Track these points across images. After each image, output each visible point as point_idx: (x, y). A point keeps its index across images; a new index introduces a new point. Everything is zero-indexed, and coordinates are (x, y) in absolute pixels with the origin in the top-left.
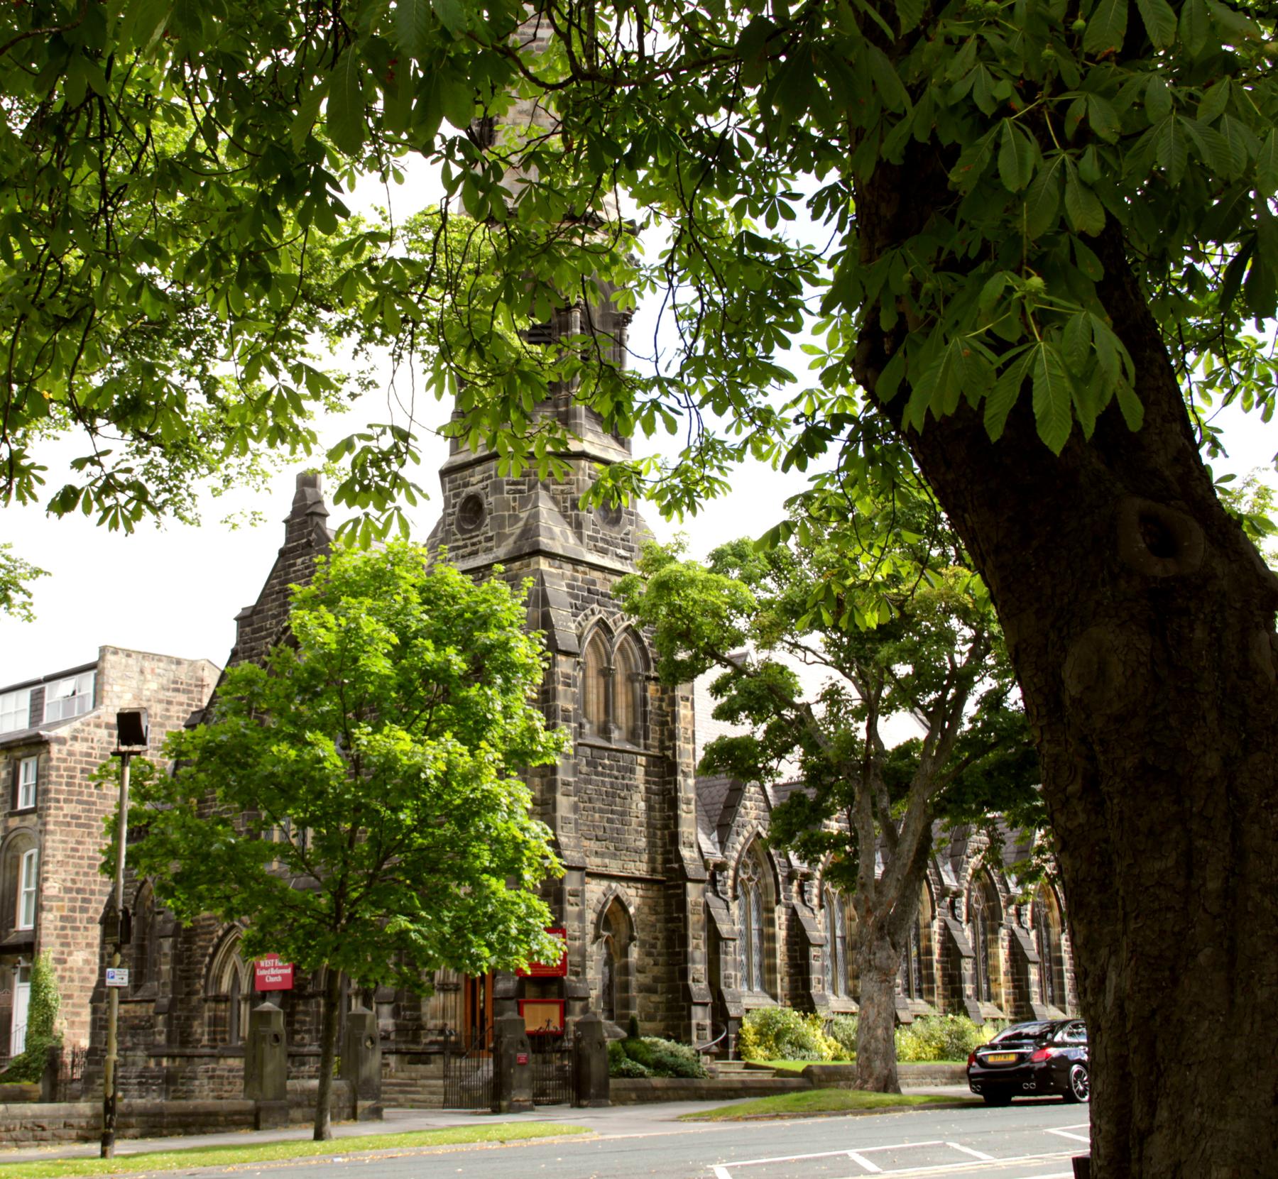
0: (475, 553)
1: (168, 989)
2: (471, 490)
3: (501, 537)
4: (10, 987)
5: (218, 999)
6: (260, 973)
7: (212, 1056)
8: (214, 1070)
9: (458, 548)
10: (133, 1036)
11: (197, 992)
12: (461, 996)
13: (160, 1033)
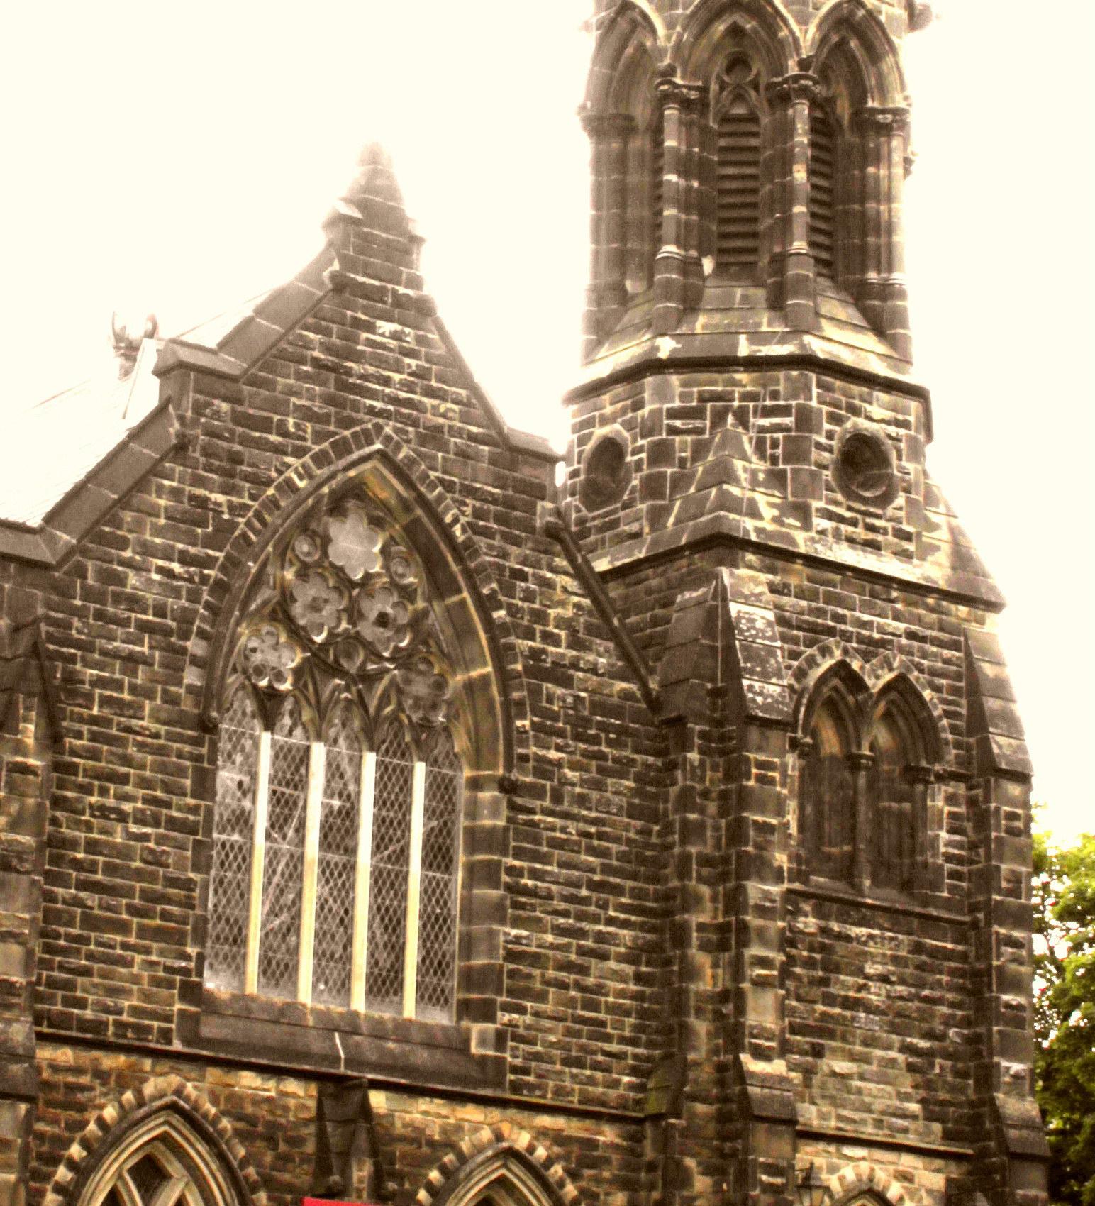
2: (863, 423)
9: (841, 519)
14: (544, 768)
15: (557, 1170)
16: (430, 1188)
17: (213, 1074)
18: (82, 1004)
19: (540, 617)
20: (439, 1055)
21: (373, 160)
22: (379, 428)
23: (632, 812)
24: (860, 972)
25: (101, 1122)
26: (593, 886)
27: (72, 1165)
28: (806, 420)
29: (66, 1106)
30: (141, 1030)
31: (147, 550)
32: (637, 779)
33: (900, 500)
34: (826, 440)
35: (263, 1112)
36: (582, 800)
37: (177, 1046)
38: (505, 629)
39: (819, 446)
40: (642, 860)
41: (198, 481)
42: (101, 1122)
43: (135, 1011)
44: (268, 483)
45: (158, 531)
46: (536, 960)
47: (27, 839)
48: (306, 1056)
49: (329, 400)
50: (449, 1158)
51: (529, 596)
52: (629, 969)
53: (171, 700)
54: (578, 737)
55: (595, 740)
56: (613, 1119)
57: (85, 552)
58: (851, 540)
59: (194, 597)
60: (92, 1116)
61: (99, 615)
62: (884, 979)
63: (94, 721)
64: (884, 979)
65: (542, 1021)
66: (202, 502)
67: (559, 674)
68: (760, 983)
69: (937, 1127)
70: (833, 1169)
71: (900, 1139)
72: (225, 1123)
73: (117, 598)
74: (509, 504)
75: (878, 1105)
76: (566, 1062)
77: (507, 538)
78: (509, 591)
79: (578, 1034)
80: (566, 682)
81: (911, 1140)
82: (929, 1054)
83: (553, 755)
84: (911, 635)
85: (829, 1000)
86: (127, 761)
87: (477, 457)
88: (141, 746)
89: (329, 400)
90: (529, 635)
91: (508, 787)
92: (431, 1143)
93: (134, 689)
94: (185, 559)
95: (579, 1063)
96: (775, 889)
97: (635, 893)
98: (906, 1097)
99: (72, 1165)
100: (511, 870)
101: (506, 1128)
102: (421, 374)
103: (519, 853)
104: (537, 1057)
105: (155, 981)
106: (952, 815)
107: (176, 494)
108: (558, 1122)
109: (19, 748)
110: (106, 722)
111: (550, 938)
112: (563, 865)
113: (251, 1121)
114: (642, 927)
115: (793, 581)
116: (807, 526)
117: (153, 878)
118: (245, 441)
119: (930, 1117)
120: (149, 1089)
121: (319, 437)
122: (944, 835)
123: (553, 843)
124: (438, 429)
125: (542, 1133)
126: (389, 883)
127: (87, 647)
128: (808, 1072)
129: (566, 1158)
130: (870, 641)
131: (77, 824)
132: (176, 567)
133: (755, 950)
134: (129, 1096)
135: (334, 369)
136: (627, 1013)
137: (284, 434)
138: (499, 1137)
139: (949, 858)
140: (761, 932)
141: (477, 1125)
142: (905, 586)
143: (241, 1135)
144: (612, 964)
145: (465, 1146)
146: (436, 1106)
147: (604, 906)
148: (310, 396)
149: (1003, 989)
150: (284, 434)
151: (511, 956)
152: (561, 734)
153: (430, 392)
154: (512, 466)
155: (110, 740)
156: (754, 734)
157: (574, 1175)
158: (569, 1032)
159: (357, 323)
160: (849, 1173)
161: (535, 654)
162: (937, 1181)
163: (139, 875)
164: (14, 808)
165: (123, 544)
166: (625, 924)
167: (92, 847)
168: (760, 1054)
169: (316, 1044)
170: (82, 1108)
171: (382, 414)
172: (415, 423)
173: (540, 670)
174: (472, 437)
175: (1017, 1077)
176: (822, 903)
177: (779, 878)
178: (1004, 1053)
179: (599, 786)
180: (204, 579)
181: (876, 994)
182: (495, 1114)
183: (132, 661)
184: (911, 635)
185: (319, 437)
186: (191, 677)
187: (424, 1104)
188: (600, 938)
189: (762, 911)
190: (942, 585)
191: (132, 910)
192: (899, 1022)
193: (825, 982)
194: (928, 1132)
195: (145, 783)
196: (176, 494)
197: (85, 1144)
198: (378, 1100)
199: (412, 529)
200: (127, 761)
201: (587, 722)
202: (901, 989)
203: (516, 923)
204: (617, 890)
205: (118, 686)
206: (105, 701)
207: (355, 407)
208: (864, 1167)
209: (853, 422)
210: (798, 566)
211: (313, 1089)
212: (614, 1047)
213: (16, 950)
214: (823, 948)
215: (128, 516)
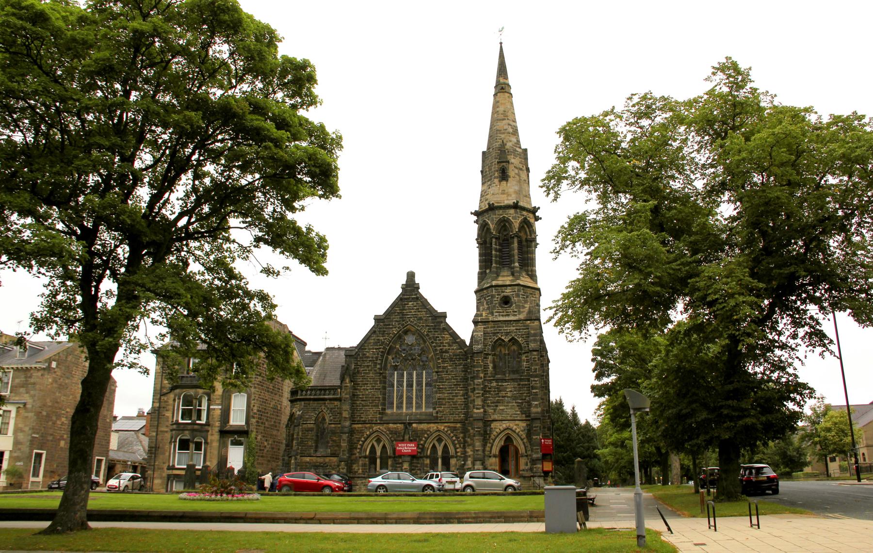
1: (346, 453)
2: (505, 294)
3: (520, 312)
4: (227, 447)
5: (365, 457)
14: (444, 368)
21: (411, 276)
28: (493, 296)
34: (497, 300)
67: (446, 352)
91: (437, 372)
126: (420, 391)
128: (495, 410)
141: (433, 427)
148: (397, 318)
160: (504, 426)
162: (525, 425)
168: (477, 409)
169: (403, 418)
173: (442, 352)
176: (497, 381)
181: (509, 394)
183: (368, 366)
186: (378, 366)
192: (514, 398)
198: (414, 425)
209: (502, 294)
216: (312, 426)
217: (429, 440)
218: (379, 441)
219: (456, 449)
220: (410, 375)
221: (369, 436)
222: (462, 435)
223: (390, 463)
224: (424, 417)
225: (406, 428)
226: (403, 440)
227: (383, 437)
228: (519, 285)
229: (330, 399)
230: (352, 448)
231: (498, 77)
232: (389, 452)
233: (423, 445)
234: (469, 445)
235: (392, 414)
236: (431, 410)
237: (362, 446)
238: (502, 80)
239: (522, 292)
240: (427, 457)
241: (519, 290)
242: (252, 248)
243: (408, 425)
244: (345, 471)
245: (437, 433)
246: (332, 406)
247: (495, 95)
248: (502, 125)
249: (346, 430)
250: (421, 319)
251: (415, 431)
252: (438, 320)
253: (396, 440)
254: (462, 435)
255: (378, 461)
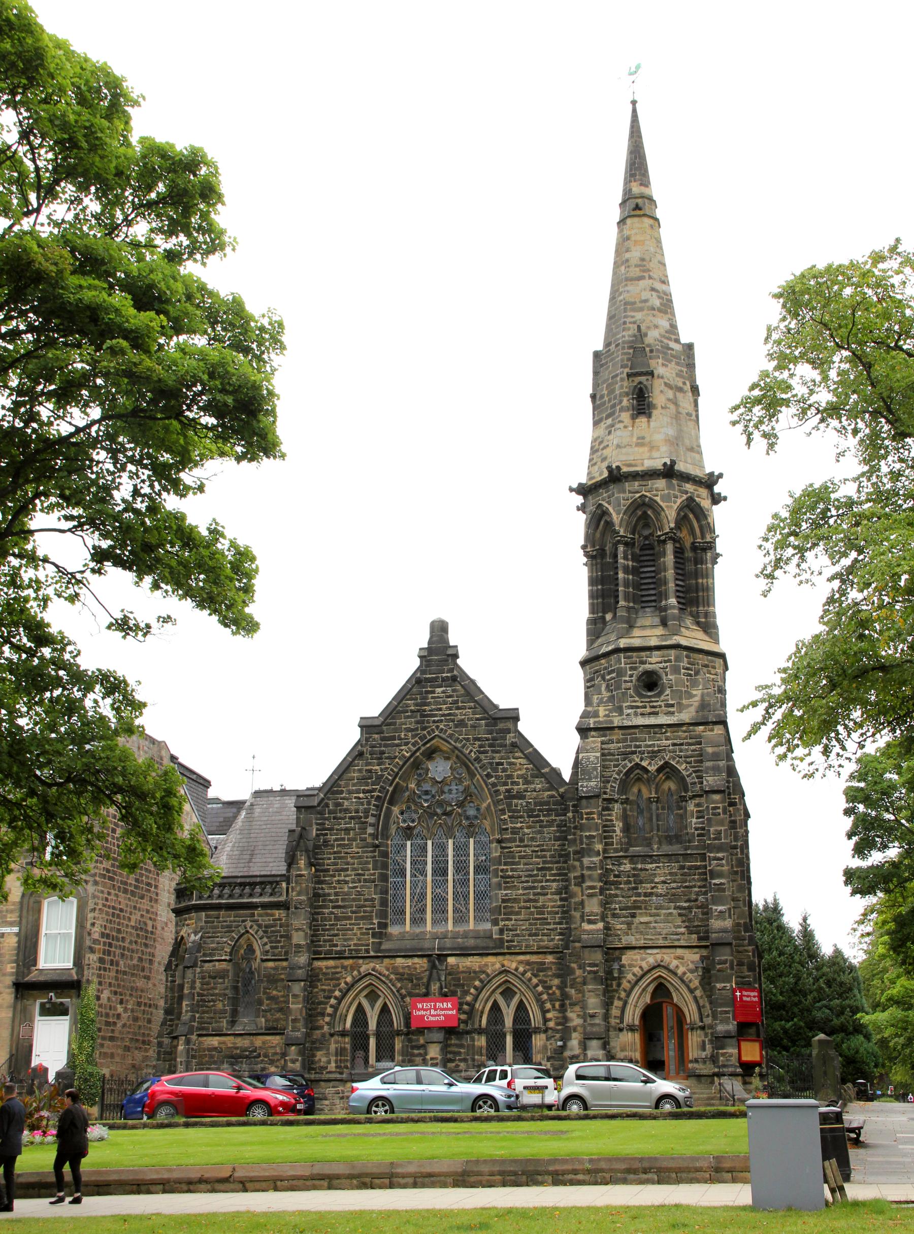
0: (656, 713)
1: (300, 1025)
3: (681, 707)
4: (32, 1020)
5: (343, 1034)
6: (416, 1013)
7: (341, 1080)
8: (343, 1092)
9: (638, 707)
10: (232, 1064)
11: (322, 1027)
12: (637, 1036)
13: (293, 1061)
14: (515, 831)
15: (529, 974)
16: (476, 988)
17: (386, 961)
18: (336, 945)
19: (510, 777)
20: (478, 941)
21: (439, 630)
22: (437, 727)
23: (557, 839)
24: (652, 882)
25: (346, 983)
26: (539, 869)
27: (336, 998)
28: (620, 673)
29: (331, 979)
30: (356, 950)
31: (350, 792)
32: (558, 826)
33: (668, 692)
34: (630, 679)
35: (407, 971)
36: (532, 839)
37: (372, 954)
38: (494, 785)
39: (626, 681)
40: (560, 856)
41: (368, 764)
42: (346, 983)
43: (355, 945)
44: (395, 757)
45: (354, 785)
46: (515, 900)
47: (303, 898)
48: (421, 950)
49: (417, 722)
50: (483, 976)
51: (504, 770)
52: (557, 897)
53: (363, 840)
54: (529, 817)
55: (538, 816)
56: (551, 953)
57: (329, 799)
58: (642, 714)
59: (369, 803)
60: (342, 981)
61: (334, 818)
62: (664, 882)
63: (335, 853)
64: (664, 882)
65: (520, 923)
66: (370, 771)
67: (520, 796)
68: (591, 896)
69: (694, 936)
70: (643, 959)
71: (677, 944)
72: (392, 976)
73: (341, 811)
74: (494, 739)
75: (664, 932)
76: (530, 935)
77: (493, 752)
78: (496, 770)
79: (536, 924)
80: (522, 797)
81: (683, 943)
82: (689, 908)
83: (519, 825)
84: (674, 745)
85: (639, 895)
86: (348, 864)
87: (480, 726)
88: (352, 858)
89: (417, 722)
90: (505, 784)
91: (499, 841)
92: (475, 972)
93: (349, 839)
94: (364, 792)
95: (536, 935)
96: (595, 859)
97: (558, 869)
98: (679, 927)
99: (336, 998)
100: (502, 870)
101: (506, 963)
102: (456, 702)
103: (506, 864)
104: (517, 935)
105: (362, 934)
106: (698, 812)
107: (360, 771)
108: (528, 957)
109: (299, 869)
110: (340, 852)
111: (521, 892)
112: (525, 864)
113: (402, 974)
114: (558, 881)
115: (615, 738)
116: (621, 714)
117: (360, 900)
118: (386, 746)
119: (691, 933)
120: (362, 970)
121: (414, 737)
122: (694, 820)
123: (521, 857)
124: (463, 720)
125: (521, 962)
127: (331, 829)
128: (629, 924)
129: (532, 969)
130: (653, 752)
131: (330, 888)
132: (361, 795)
133: (589, 884)
134: (355, 973)
135: (418, 711)
136: (557, 913)
137: (400, 739)
138: (503, 966)
139: (696, 829)
140: (590, 877)
141: (493, 963)
142: (669, 726)
143: (399, 980)
144: (549, 896)
145: (489, 971)
146: (477, 959)
147: (545, 875)
148: (411, 723)
149: (712, 878)
150: (400, 739)
151: (504, 901)
152: (521, 817)
153: (458, 708)
154: (495, 725)
155: (340, 858)
156: (584, 802)
157: (535, 976)
158: (530, 924)
159: (428, 692)
160: (651, 960)
161: (508, 791)
162: (697, 957)
163: (354, 900)
164: (298, 889)
165: (342, 792)
166: (554, 881)
167: (336, 894)
168: (590, 922)
169: (427, 945)
170: (338, 979)
171: (438, 721)
172: (453, 721)
173: (510, 796)
174: (477, 719)
175: (721, 912)
176: (633, 858)
177: (598, 854)
178: (714, 904)
179: (540, 832)
180: (372, 797)
181: (661, 889)
182: (500, 958)
183: (347, 830)
184: (674, 745)
185: (414, 737)
186: (370, 830)
187: (470, 959)
188: (543, 888)
189: (589, 868)
190: (687, 721)
191: (353, 912)
192: (673, 897)
193: (636, 888)
194: (689, 939)
195: (354, 869)
196: (360, 771)
197: (340, 990)
198: (451, 960)
199: (457, 757)
200: (348, 864)
201: (534, 810)
202: (674, 885)
203: (506, 888)
204: (550, 869)
205: (343, 839)
206: (338, 845)
207: (428, 722)
208: (659, 957)
209: (642, 668)
210: (617, 731)
211: (425, 960)
212: (552, 926)
213: (301, 933)
214: (634, 875)
215: (342, 783)
216: (224, 965)
217: (484, 994)
218: (372, 996)
219: (544, 1012)
220: (441, 849)
221: (350, 987)
222: (556, 981)
223: (398, 1044)
224: (471, 942)
225: (433, 967)
226: (427, 994)
227: (382, 987)
228: (677, 646)
229: (265, 906)
230: (312, 1014)
231: (627, 182)
232: (397, 1022)
233: (472, 1005)
234: (573, 1005)
235: (402, 936)
236: (488, 926)
237: (336, 1008)
238: (636, 189)
239: (684, 663)
240: (480, 1031)
241: (678, 659)
242: (88, 574)
243: (437, 959)
244: (297, 1066)
245: (502, 978)
246: (265, 920)
247: (622, 222)
248: (638, 291)
249: (300, 973)
250: (461, 724)
251: (452, 972)
252: (501, 726)
253: (410, 994)
254: (556, 981)
255: (372, 1042)
